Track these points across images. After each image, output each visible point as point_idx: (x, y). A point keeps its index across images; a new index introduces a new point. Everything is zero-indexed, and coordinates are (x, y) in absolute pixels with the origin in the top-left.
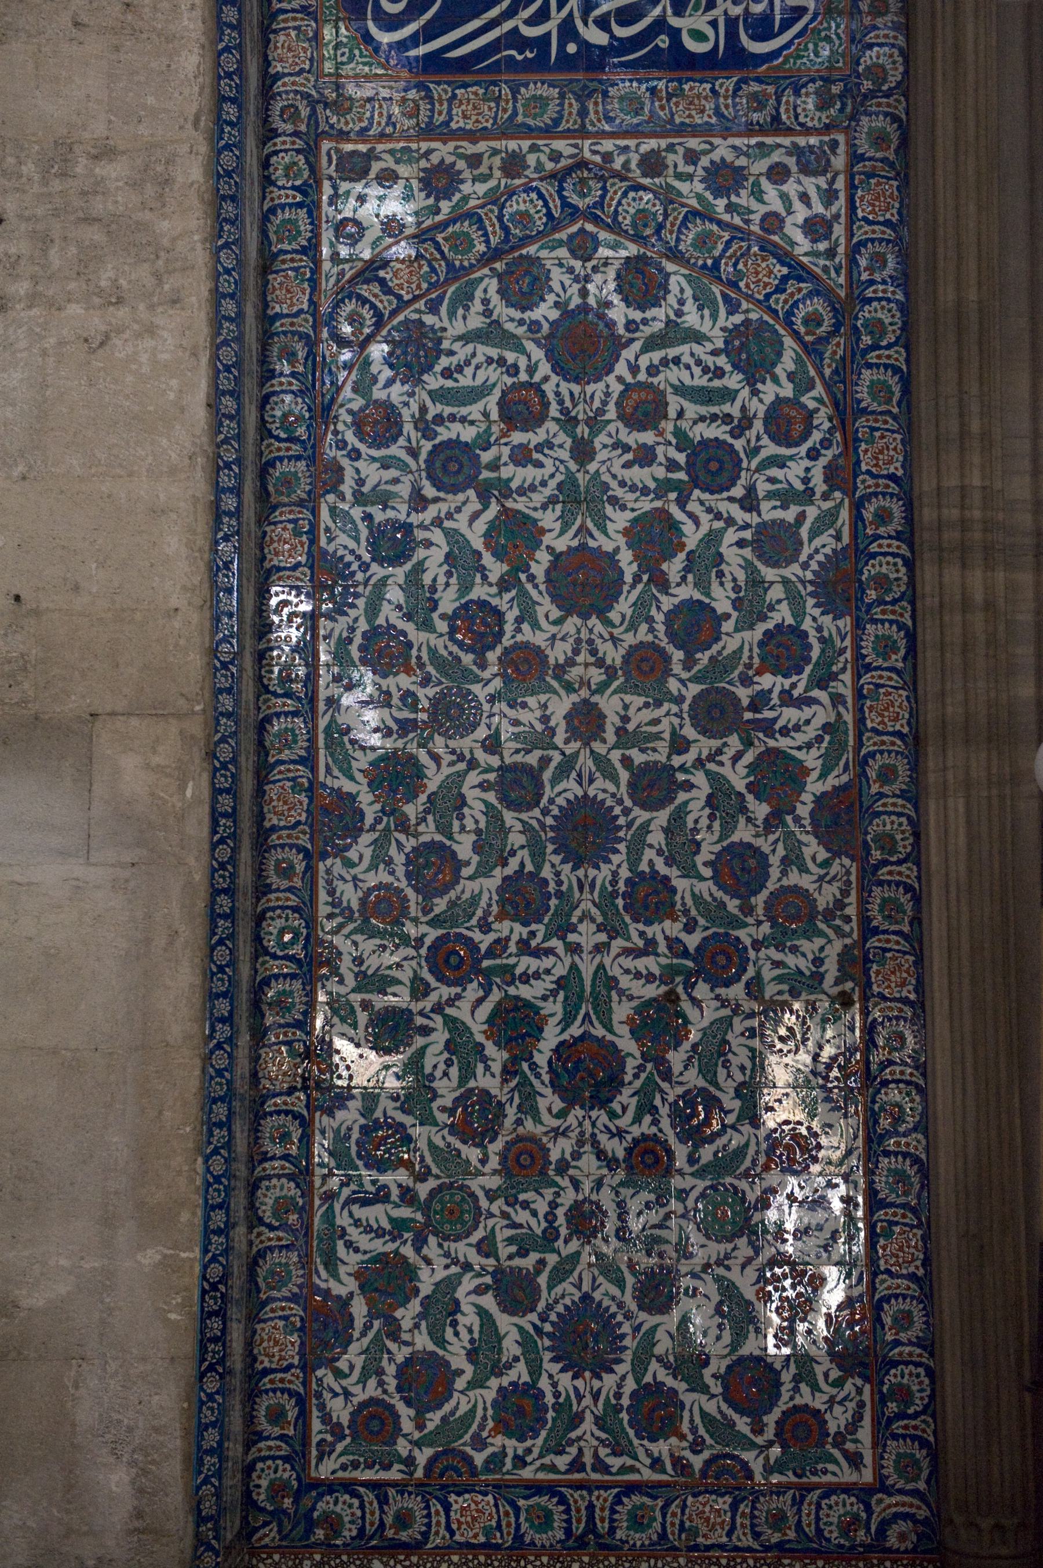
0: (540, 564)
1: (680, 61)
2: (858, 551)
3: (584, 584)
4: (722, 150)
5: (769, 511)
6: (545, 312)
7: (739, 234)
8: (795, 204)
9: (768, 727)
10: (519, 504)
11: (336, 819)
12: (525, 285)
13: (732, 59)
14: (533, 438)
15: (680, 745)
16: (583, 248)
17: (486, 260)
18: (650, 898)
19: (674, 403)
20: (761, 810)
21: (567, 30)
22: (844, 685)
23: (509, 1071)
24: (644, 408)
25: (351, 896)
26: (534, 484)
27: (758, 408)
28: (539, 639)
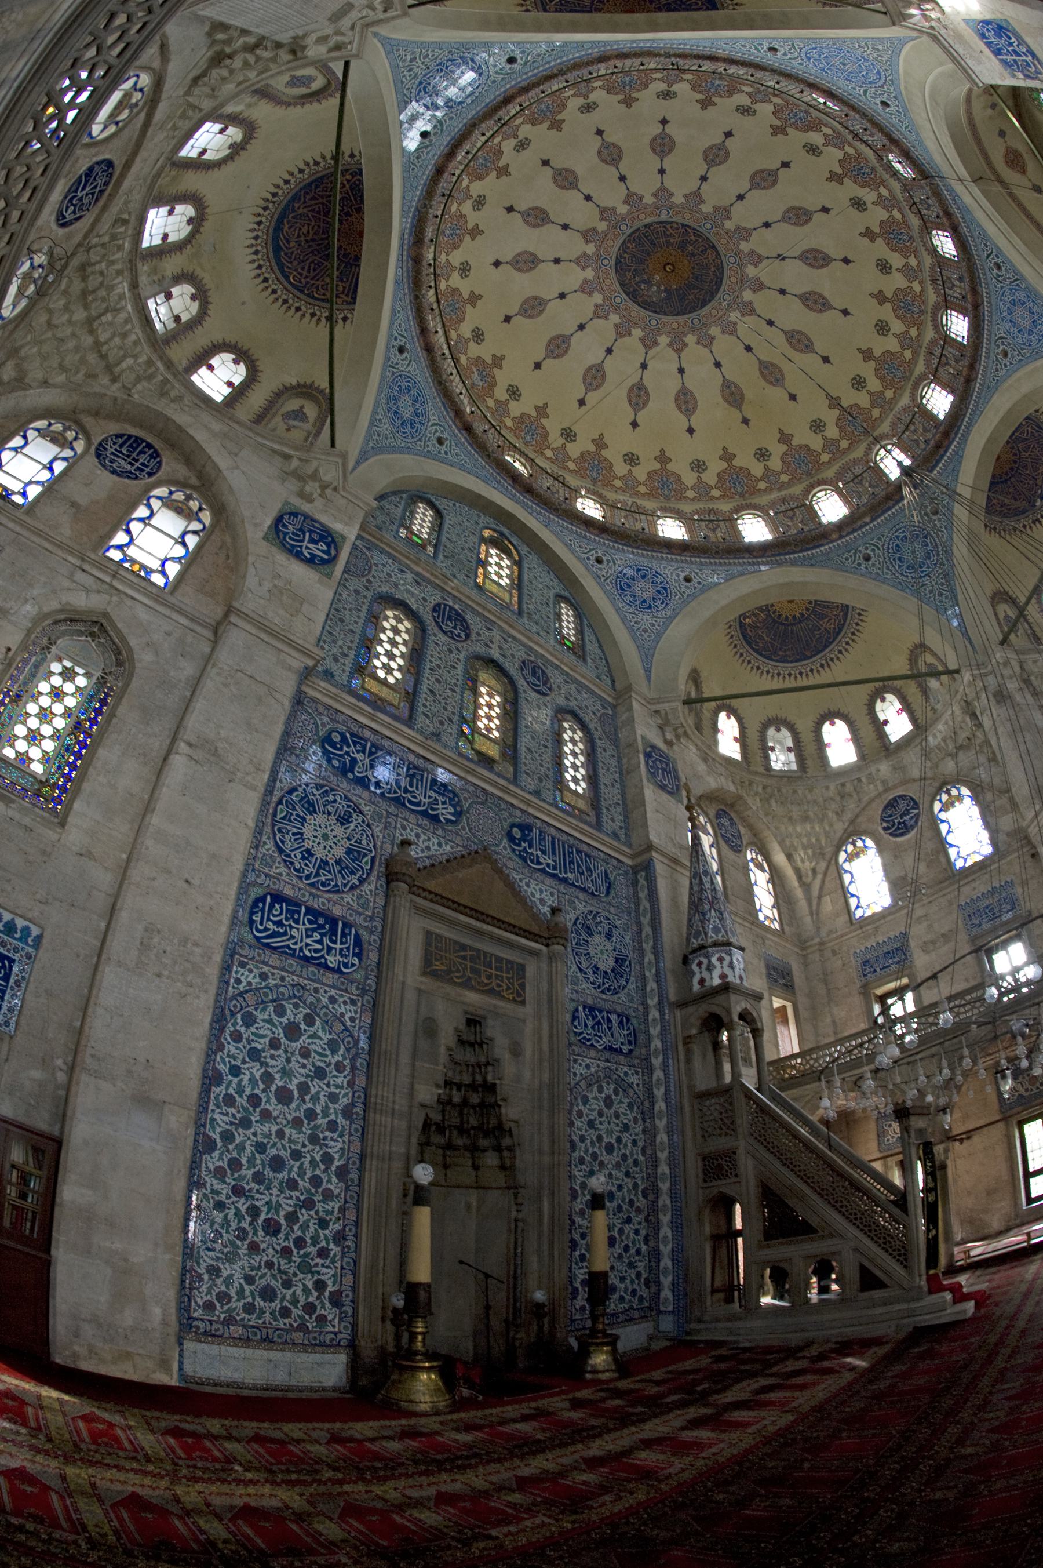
0: (273, 1088)
2: (353, 1104)
3: (284, 1096)
4: (333, 992)
5: (333, 1089)
6: (284, 1020)
7: (334, 1015)
8: (348, 1011)
9: (326, 1146)
10: (270, 1070)
12: (280, 1012)
13: (338, 971)
14: (276, 1053)
15: (304, 1146)
17: (274, 1001)
18: (292, 1184)
19: (313, 1054)
20: (323, 1167)
21: (301, 949)
22: (346, 1138)
23: (251, 1224)
24: (305, 1053)
25: (212, 1167)
26: (275, 1066)
27: (333, 1062)
28: (270, 1108)
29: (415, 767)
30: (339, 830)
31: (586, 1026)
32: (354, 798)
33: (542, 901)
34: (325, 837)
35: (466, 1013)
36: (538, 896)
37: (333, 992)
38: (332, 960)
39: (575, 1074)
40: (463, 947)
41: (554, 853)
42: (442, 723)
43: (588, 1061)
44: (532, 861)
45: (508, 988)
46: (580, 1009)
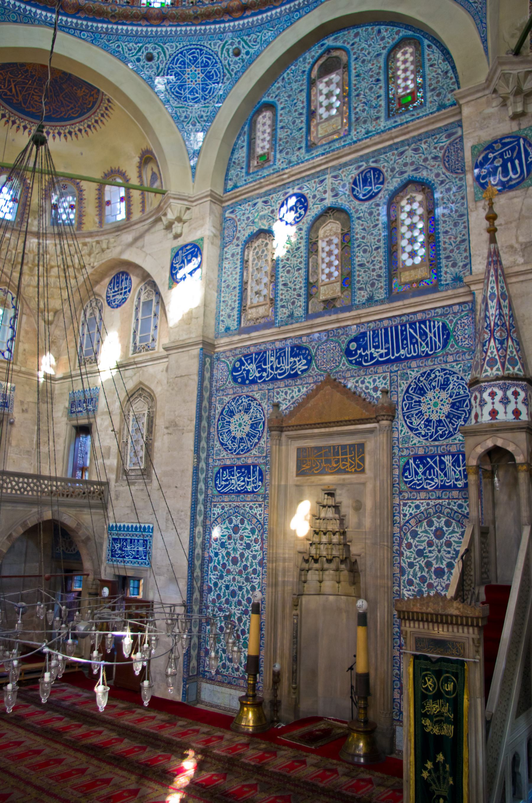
1: (247, 492)
2: (263, 559)
3: (235, 561)
5: (254, 553)
11: (210, 590)
12: (231, 522)
13: (253, 492)
16: (236, 517)
29: (280, 349)
30: (246, 417)
31: (417, 473)
32: (250, 394)
33: (375, 389)
34: (240, 425)
35: (323, 490)
36: (372, 386)
37: (251, 504)
38: (249, 488)
39: (405, 515)
40: (319, 449)
41: (387, 342)
42: (293, 303)
43: (417, 502)
44: (366, 361)
45: (351, 464)
46: (411, 461)
